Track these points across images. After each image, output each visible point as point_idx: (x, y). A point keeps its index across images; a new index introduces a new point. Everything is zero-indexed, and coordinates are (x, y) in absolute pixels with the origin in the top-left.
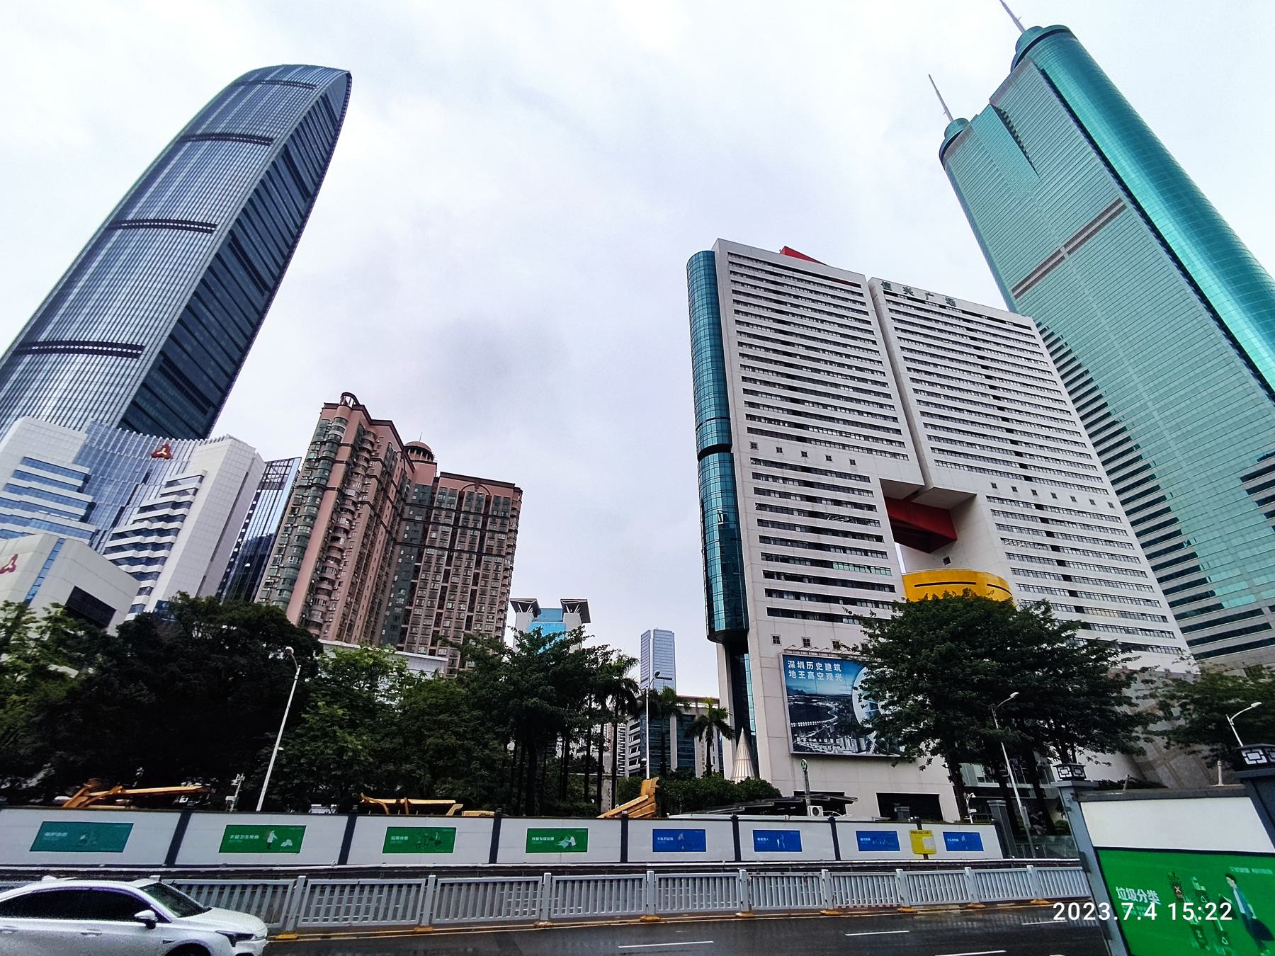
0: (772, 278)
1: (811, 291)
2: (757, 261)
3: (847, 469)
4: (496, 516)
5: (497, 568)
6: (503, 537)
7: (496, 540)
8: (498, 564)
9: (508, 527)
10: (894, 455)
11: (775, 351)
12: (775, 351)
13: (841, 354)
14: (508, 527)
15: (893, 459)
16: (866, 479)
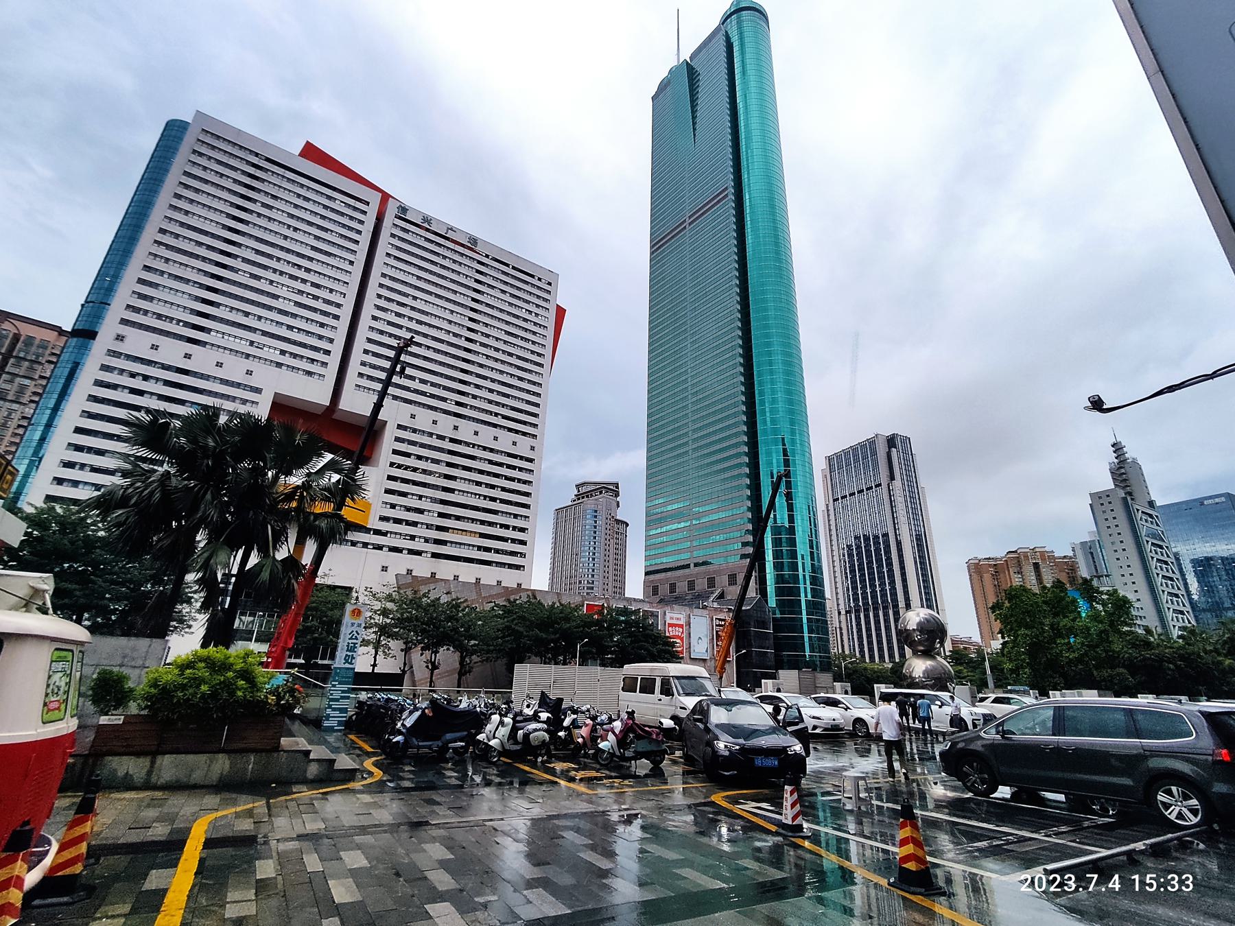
0: (252, 170)
1: (299, 196)
2: (241, 147)
3: (239, 377)
4: (24, 359)
5: (10, 414)
6: (27, 382)
7: (16, 384)
8: (11, 411)
9: (38, 373)
10: (309, 373)
11: (210, 248)
12: (210, 248)
13: (300, 267)
14: (38, 373)
15: (306, 377)
16: (258, 391)
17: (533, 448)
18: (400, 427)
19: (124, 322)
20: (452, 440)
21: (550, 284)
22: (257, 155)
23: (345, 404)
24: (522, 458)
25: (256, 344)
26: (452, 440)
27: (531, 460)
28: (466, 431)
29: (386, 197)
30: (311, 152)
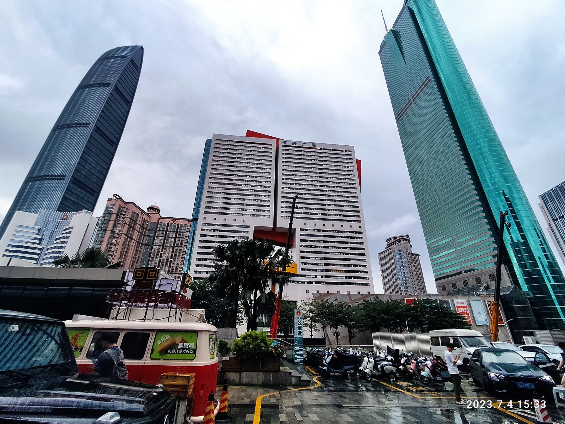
0: (232, 147)
1: (248, 151)
4: (181, 232)
5: (180, 251)
6: (183, 239)
7: (180, 241)
8: (180, 250)
9: (185, 236)
10: (264, 216)
11: (225, 179)
12: (225, 179)
13: (253, 176)
14: (185, 236)
16: (248, 227)
17: (360, 227)
18: (301, 230)
19: (205, 212)
20: (324, 231)
21: (351, 151)
22: (233, 141)
23: (278, 225)
24: (356, 232)
25: (245, 210)
26: (324, 231)
27: (361, 233)
28: (329, 225)
29: (277, 140)
30: (250, 134)
